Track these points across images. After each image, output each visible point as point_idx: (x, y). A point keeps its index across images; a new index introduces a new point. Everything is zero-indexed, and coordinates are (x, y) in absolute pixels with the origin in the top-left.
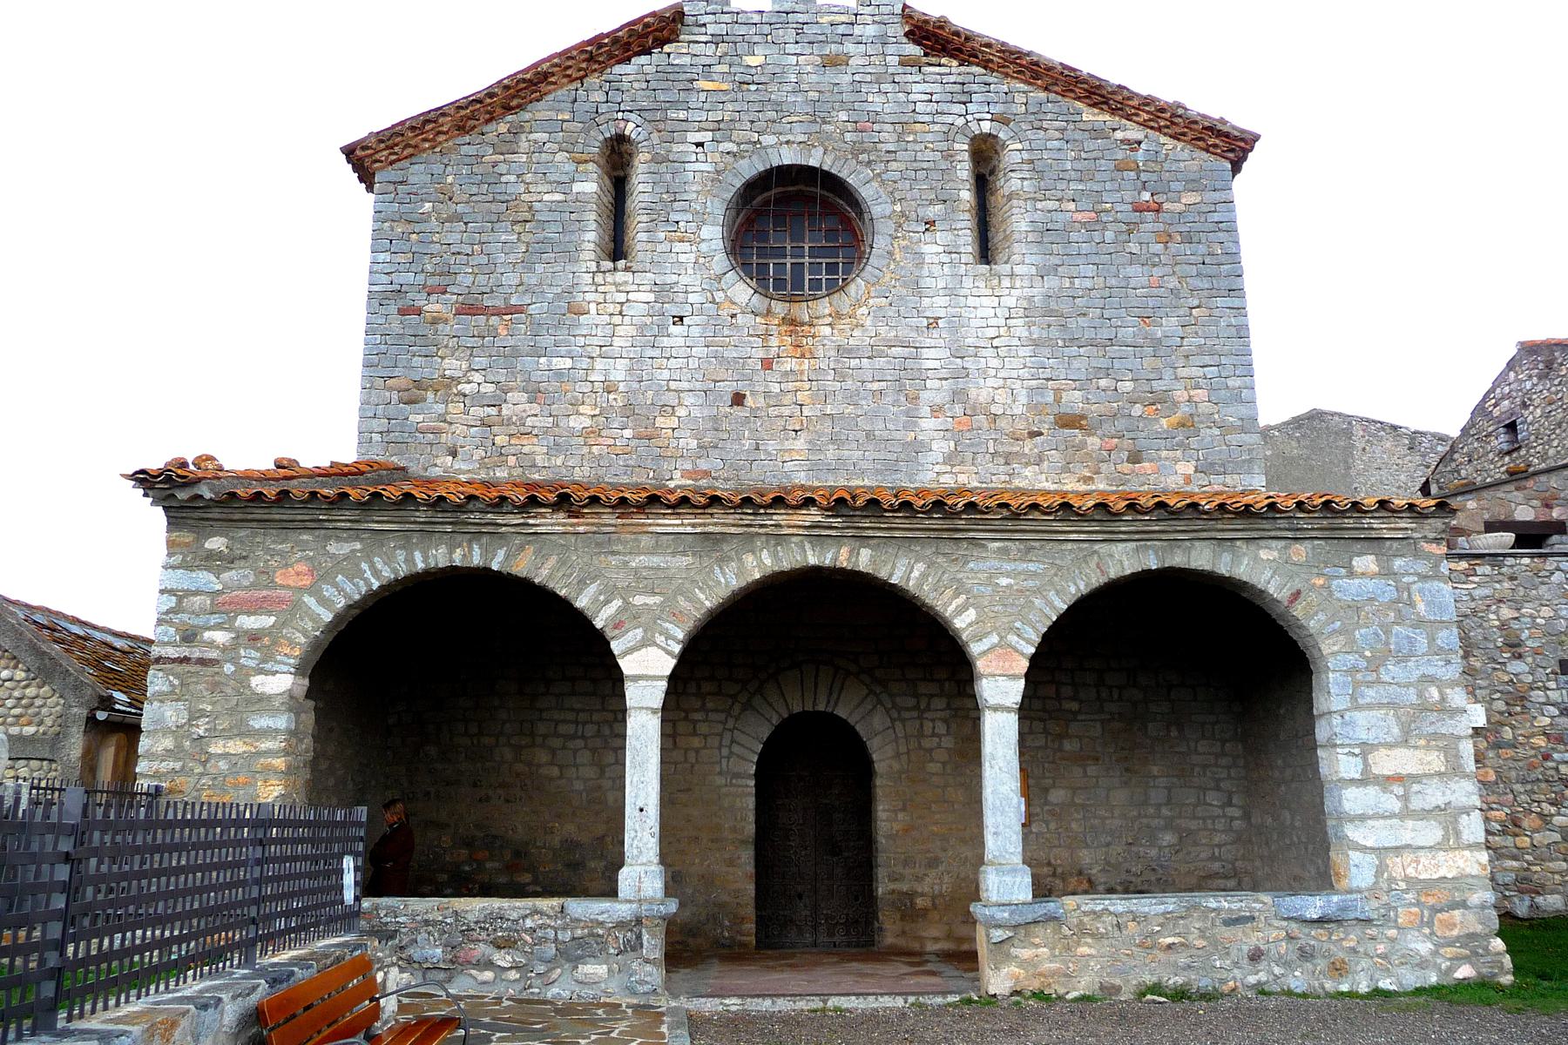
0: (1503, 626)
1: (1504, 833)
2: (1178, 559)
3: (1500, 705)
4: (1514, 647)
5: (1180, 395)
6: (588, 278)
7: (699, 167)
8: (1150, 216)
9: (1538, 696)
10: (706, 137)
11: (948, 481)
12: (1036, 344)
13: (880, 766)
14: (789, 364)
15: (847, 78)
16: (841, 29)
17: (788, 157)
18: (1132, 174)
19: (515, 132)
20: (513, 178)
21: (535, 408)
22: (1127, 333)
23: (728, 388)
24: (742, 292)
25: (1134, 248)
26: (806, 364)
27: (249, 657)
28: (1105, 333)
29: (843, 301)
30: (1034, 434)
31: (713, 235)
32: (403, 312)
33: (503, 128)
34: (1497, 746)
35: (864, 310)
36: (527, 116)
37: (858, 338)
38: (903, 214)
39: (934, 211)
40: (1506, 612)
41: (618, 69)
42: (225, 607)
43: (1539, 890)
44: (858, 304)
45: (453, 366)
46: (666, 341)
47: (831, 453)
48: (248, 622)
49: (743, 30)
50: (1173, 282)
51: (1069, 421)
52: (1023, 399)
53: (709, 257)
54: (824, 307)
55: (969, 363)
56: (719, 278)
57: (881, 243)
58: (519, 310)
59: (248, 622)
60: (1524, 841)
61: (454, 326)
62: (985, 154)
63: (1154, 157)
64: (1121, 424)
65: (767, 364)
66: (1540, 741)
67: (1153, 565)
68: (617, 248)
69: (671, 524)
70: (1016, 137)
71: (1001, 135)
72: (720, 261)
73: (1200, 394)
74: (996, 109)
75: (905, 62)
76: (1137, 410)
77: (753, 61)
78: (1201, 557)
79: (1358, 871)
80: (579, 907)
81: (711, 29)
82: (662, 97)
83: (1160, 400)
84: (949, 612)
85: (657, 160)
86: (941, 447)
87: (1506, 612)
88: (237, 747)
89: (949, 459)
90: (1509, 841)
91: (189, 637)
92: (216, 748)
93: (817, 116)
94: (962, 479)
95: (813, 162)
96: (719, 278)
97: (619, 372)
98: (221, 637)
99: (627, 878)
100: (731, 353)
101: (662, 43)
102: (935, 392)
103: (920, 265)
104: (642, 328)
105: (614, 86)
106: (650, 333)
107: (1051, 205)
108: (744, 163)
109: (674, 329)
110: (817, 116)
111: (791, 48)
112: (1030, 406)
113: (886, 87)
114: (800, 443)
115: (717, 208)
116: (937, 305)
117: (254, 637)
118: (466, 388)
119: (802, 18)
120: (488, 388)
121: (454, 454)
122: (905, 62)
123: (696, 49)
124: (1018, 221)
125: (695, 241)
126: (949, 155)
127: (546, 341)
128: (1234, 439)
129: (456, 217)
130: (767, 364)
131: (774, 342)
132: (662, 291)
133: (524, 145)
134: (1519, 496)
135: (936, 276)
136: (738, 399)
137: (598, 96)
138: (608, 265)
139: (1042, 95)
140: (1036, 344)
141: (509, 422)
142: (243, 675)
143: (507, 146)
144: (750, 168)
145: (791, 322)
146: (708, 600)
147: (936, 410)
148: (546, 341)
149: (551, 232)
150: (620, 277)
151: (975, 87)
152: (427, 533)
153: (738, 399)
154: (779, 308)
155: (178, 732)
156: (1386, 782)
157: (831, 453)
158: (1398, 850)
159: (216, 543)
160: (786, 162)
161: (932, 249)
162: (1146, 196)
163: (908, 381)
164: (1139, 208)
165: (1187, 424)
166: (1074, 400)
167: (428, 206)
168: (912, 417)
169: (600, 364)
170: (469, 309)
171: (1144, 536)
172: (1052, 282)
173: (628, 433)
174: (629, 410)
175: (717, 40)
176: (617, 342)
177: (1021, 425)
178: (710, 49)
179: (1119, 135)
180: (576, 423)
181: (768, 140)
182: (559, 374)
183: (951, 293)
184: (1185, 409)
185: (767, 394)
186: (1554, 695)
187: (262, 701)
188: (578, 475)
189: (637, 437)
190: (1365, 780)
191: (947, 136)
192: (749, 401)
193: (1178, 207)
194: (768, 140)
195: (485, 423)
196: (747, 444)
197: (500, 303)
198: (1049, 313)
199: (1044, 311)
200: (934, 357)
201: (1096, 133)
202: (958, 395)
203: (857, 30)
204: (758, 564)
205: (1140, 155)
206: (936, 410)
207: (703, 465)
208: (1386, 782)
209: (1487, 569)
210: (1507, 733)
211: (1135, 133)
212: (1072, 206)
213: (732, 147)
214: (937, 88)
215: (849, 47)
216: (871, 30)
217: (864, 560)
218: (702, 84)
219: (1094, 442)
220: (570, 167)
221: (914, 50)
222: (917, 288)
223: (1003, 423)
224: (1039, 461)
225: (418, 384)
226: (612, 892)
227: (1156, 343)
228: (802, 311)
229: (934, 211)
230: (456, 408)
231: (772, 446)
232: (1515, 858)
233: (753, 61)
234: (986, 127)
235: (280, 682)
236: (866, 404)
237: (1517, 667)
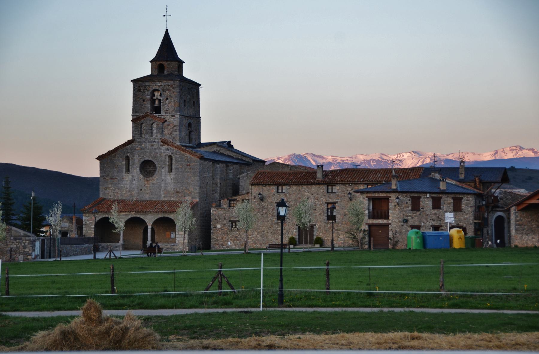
0: (224, 216)
1: (221, 239)
2: (164, 216)
3: (222, 225)
4: (225, 219)
5: (190, 189)
6: (124, 175)
7: (137, 160)
8: (188, 166)
9: (227, 224)
10: (137, 156)
11: (164, 199)
12: (174, 183)
13: (156, 231)
14: (147, 185)
15: (154, 148)
16: (154, 141)
17: (147, 159)
18: (187, 161)
19: (115, 155)
20: (115, 162)
21: (119, 191)
22: (185, 181)
23: (140, 188)
24: (142, 176)
25: (186, 170)
26: (149, 185)
27: (91, 224)
28: (182, 181)
29: (153, 177)
30: (173, 194)
31: (138, 169)
32: (104, 179)
33: (114, 154)
34: (222, 230)
35: (155, 179)
36: (117, 153)
37: (154, 182)
38: (160, 166)
39: (164, 166)
40: (224, 215)
41: (127, 147)
42: (88, 220)
43: (223, 245)
44: (154, 178)
45: (110, 186)
46: (133, 183)
47: (151, 196)
48: (90, 222)
49: (142, 141)
50: (190, 175)
51: (178, 192)
52: (172, 190)
53: (138, 172)
54: (151, 178)
55: (167, 185)
56: (139, 175)
57: (157, 170)
58: (117, 179)
59: (90, 222)
60: (223, 240)
61: (109, 181)
62: (171, 158)
63: (190, 158)
64: (183, 193)
65: (144, 185)
66: (226, 229)
67: (162, 216)
68: (128, 170)
69: (123, 213)
70: (173, 156)
71: (172, 155)
72: (139, 172)
73: (192, 189)
74: (171, 152)
75: (161, 145)
76: (185, 191)
77: (143, 145)
78: (166, 216)
79: (177, 242)
80: (117, 244)
81: (138, 141)
82: (132, 150)
83: (188, 190)
84: (145, 220)
85: (132, 159)
86: (163, 196)
87: (224, 215)
88: (90, 231)
89: (164, 197)
90: (221, 240)
91: (86, 223)
92: (89, 232)
93: (150, 153)
94: (165, 199)
95: (150, 159)
96: (139, 175)
97: (128, 186)
98: (88, 223)
99: (120, 242)
100: (140, 184)
101: (132, 143)
102: (163, 189)
103: (162, 173)
104: (131, 181)
105: (127, 149)
106: (131, 182)
107: (177, 165)
108: (142, 160)
109: (134, 181)
110: (150, 153)
111: (148, 143)
112: (173, 190)
113: (159, 149)
114: (148, 195)
115: (139, 166)
116: (163, 178)
117: (91, 223)
118: (111, 188)
119: (149, 139)
120: (114, 188)
121: (110, 196)
122: (161, 145)
123: (136, 144)
124: (173, 167)
125: (137, 170)
126: (166, 158)
127: (120, 182)
128: (195, 195)
129: (109, 167)
130: (144, 185)
131: (145, 183)
132: (132, 176)
133: (116, 157)
134: (247, 196)
135: (163, 175)
136: (141, 190)
137: (125, 150)
138: (126, 173)
139: (177, 150)
140: (174, 183)
141: (116, 192)
142: (90, 226)
143: (115, 157)
144: (142, 160)
145: (147, 180)
146: (126, 220)
147: (163, 191)
148: (120, 182)
149: (120, 169)
150: (128, 174)
151: (169, 149)
152: (104, 214)
153: (141, 190)
154: (146, 178)
155: (86, 230)
156: (180, 235)
157: (151, 196)
158: (180, 240)
159: (87, 215)
160: (147, 159)
161: (163, 171)
162: (188, 164)
163: (160, 187)
164: (187, 165)
165: (191, 193)
166: (178, 190)
167: (106, 165)
168: (160, 192)
169: (126, 186)
170: (111, 179)
171: (161, 214)
172: (176, 175)
173: (129, 194)
174: (129, 191)
175: (139, 142)
176: (128, 183)
177: (172, 193)
178: (138, 144)
179: (186, 155)
180: (124, 192)
181: (145, 156)
182: (121, 187)
183: (165, 176)
184: (190, 191)
185: (144, 189)
186: (228, 224)
187: (92, 228)
188: (124, 199)
189: (130, 194)
190: (178, 234)
191: (166, 156)
192: (142, 190)
193: (192, 165)
194: (145, 156)
195: (114, 193)
196: (142, 195)
197: (114, 178)
198: (176, 179)
199: (176, 179)
200: (163, 185)
201: (183, 155)
202: (165, 189)
203: (155, 141)
204: (130, 216)
205: (188, 158)
206: (163, 191)
207: (137, 198)
208: (180, 235)
209: (223, 210)
210: (223, 229)
211: (187, 155)
212: (179, 165)
213: (140, 157)
214: (165, 149)
215: (154, 143)
216: (157, 141)
217: (139, 216)
218: (137, 149)
219: (180, 195)
220: (122, 160)
221: (162, 144)
222: (161, 176)
223: (170, 193)
224: (174, 197)
225: (106, 188)
226: (118, 242)
227: (188, 183)
228: (148, 179)
229: (164, 166)
230: (110, 191)
231: (145, 195)
232: (222, 242)
233: (143, 145)
234: (170, 154)
235: (93, 226)
236: (155, 190)
237: (225, 221)
